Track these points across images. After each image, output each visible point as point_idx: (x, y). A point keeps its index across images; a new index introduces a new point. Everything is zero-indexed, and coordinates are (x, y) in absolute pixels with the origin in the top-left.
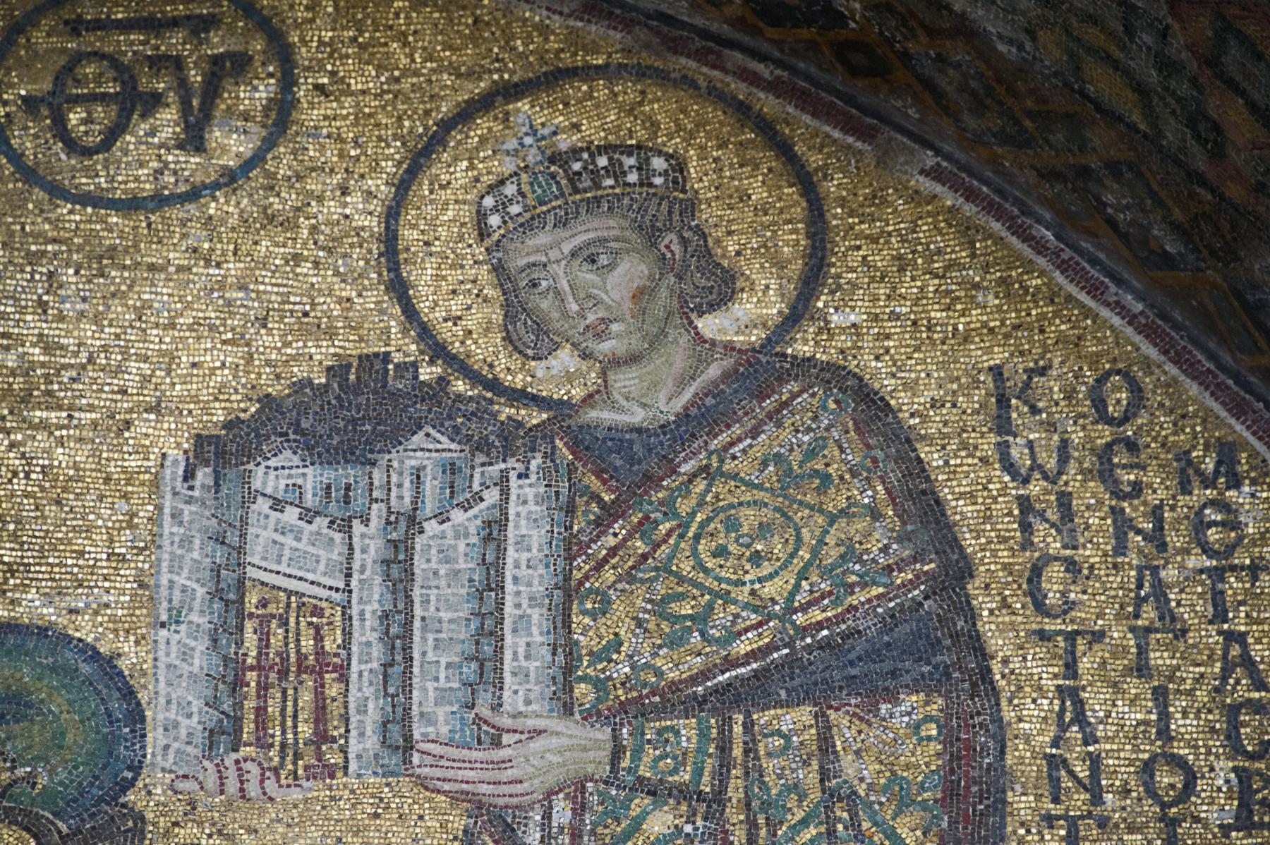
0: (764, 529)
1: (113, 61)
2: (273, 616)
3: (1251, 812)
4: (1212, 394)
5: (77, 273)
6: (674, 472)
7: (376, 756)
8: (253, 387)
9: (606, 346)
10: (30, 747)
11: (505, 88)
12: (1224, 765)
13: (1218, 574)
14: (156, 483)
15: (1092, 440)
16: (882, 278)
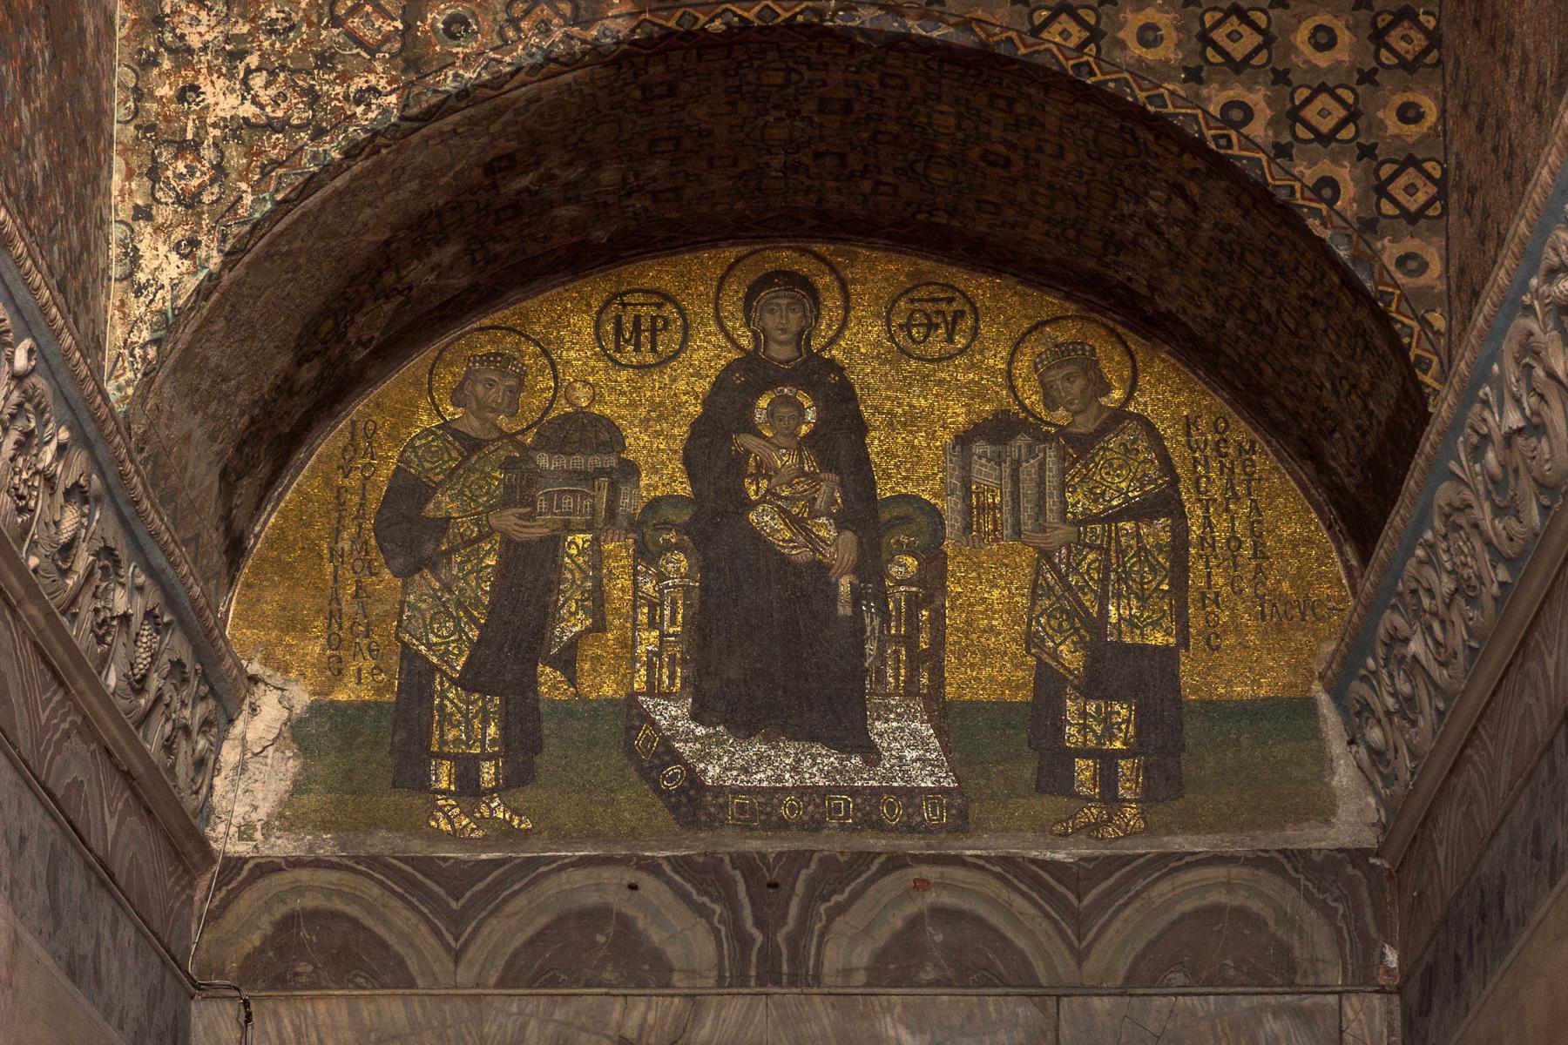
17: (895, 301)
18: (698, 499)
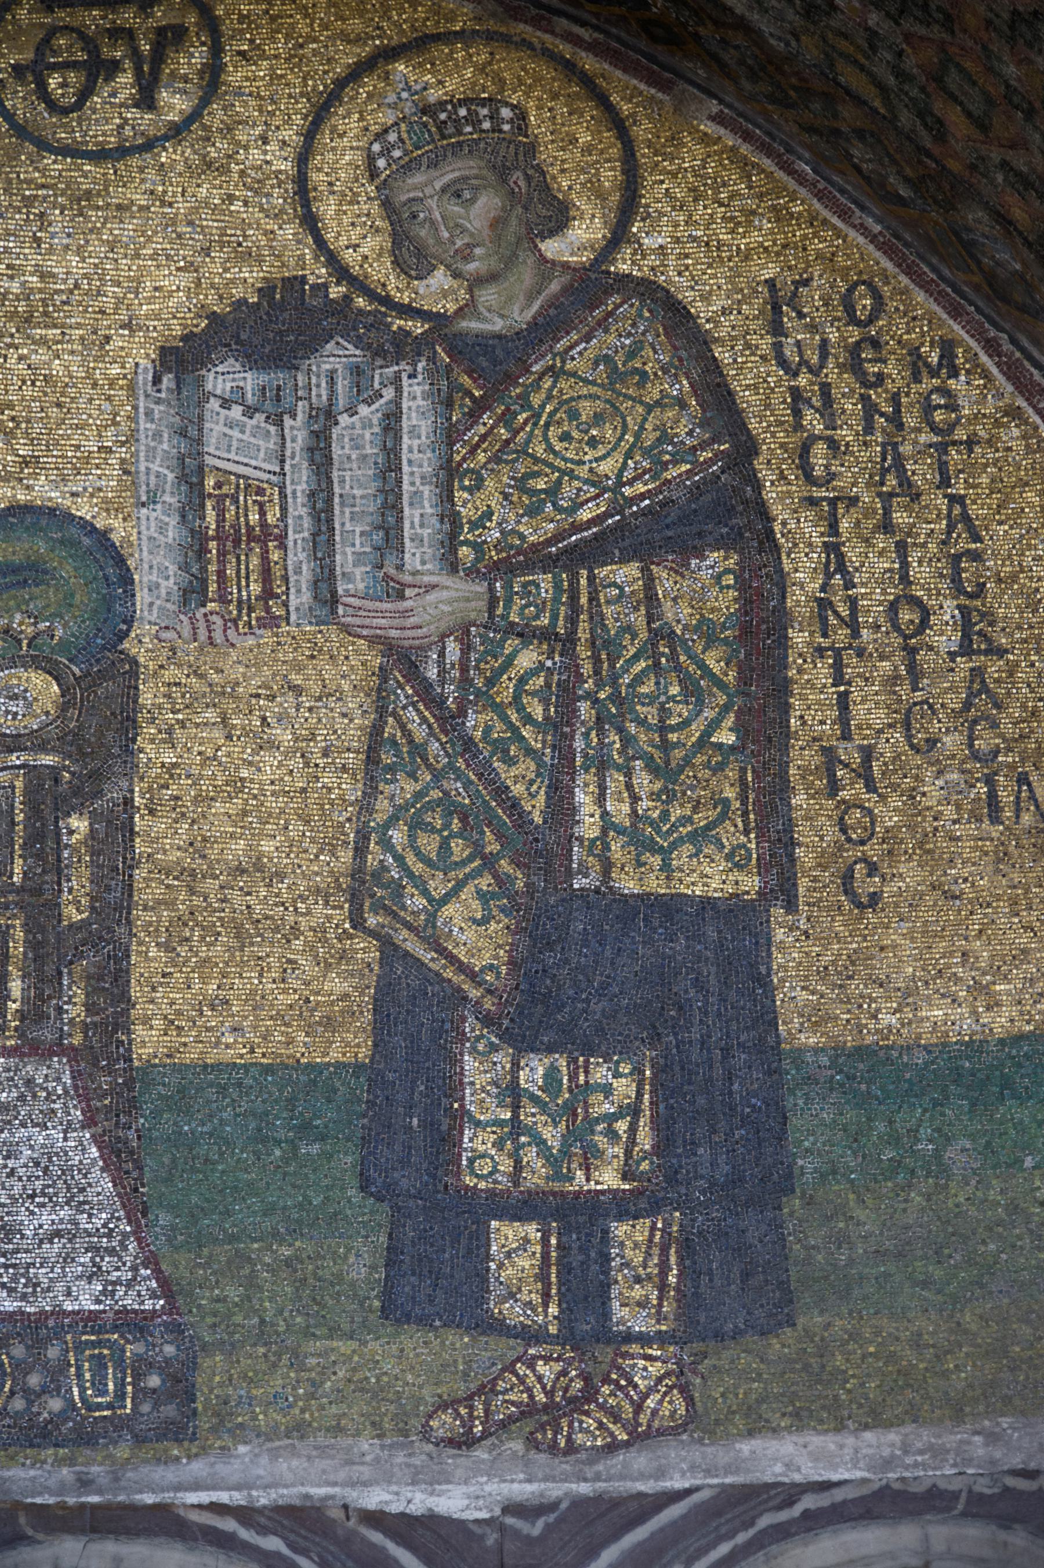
0: (598, 419)
1: (82, 35)
2: (227, 496)
3: (971, 641)
4: (936, 300)
5: (62, 213)
6: (527, 371)
7: (310, 608)
8: (202, 306)
9: (472, 267)
10: (48, 606)
11: (385, 51)
12: (949, 604)
13: (942, 448)
14: (132, 388)
15: (845, 339)
16: (681, 207)
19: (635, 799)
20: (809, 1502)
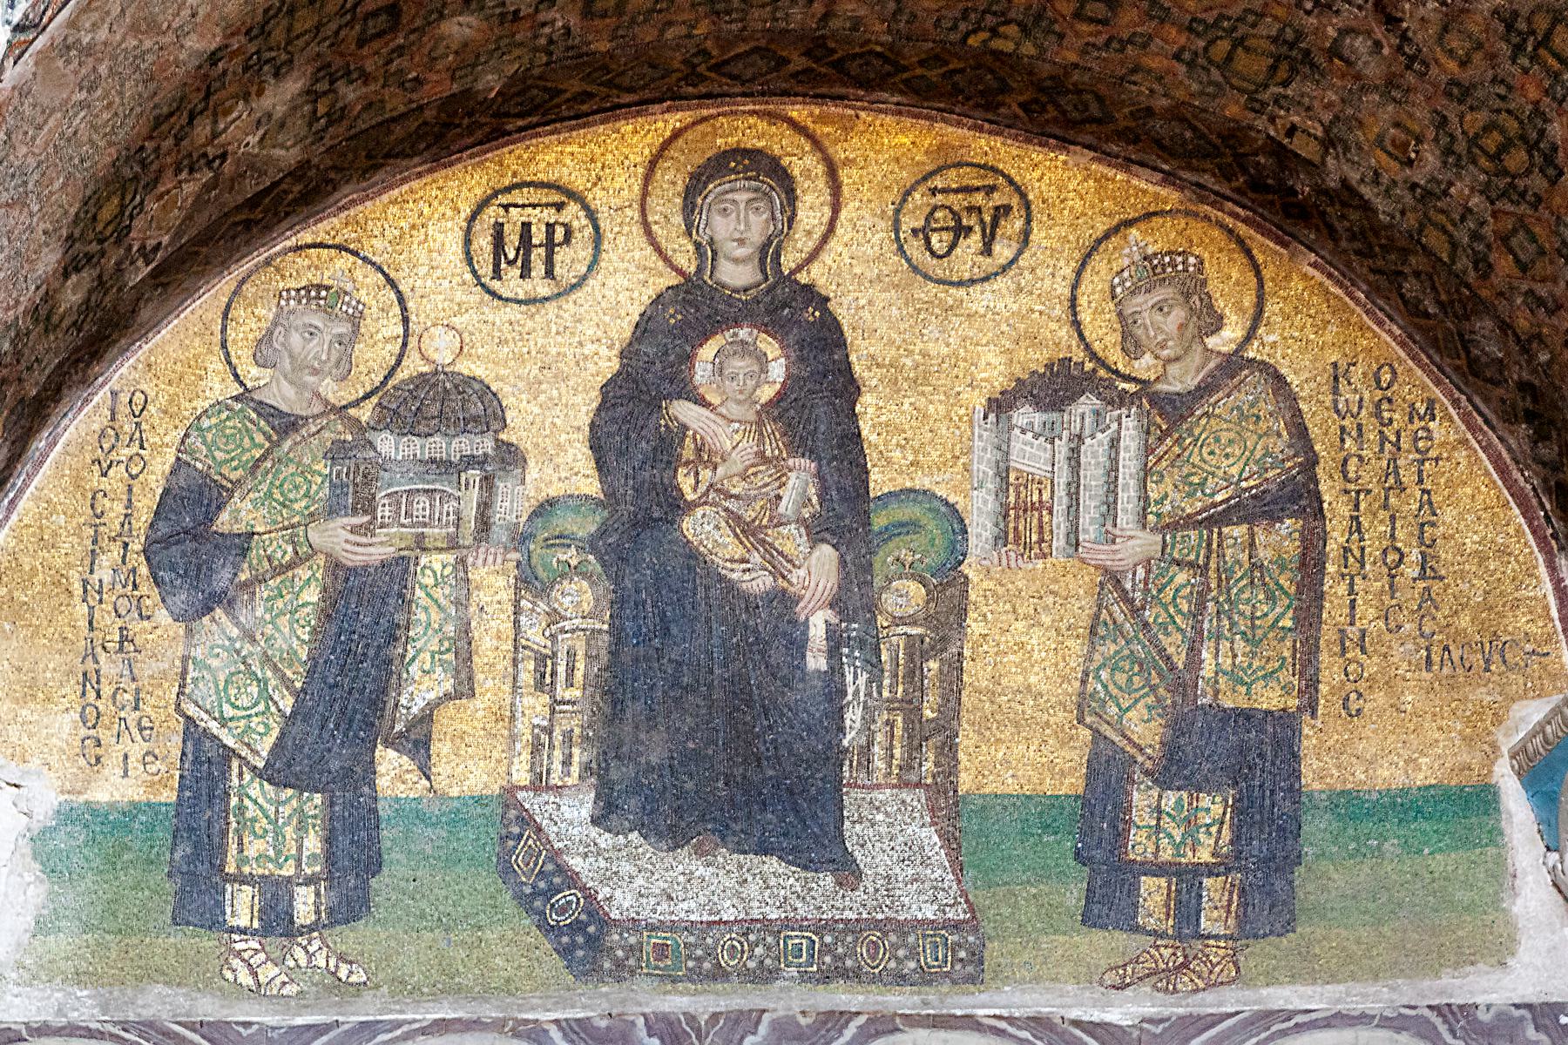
14: (971, 421)
17: (908, 193)
18: (611, 497)
19: (1235, 656)
20: (1299, 1019)
